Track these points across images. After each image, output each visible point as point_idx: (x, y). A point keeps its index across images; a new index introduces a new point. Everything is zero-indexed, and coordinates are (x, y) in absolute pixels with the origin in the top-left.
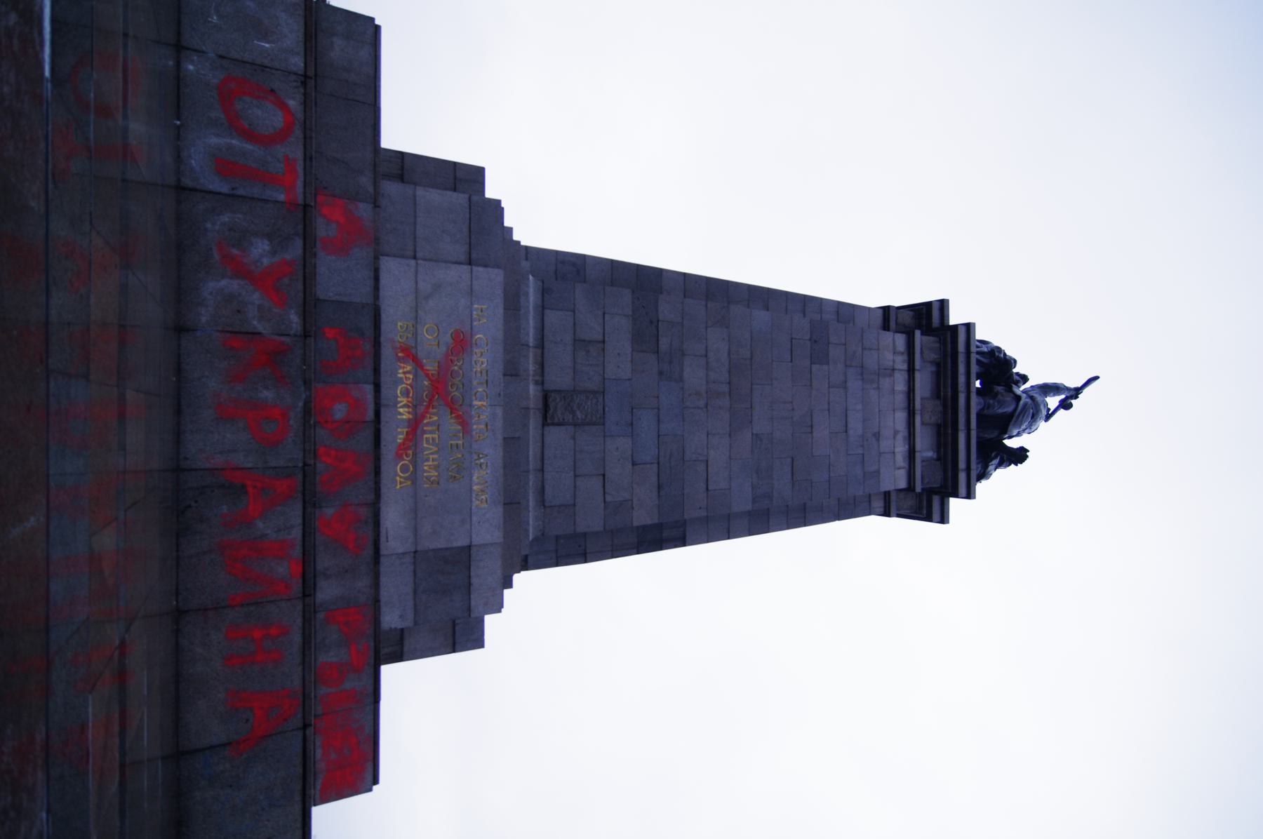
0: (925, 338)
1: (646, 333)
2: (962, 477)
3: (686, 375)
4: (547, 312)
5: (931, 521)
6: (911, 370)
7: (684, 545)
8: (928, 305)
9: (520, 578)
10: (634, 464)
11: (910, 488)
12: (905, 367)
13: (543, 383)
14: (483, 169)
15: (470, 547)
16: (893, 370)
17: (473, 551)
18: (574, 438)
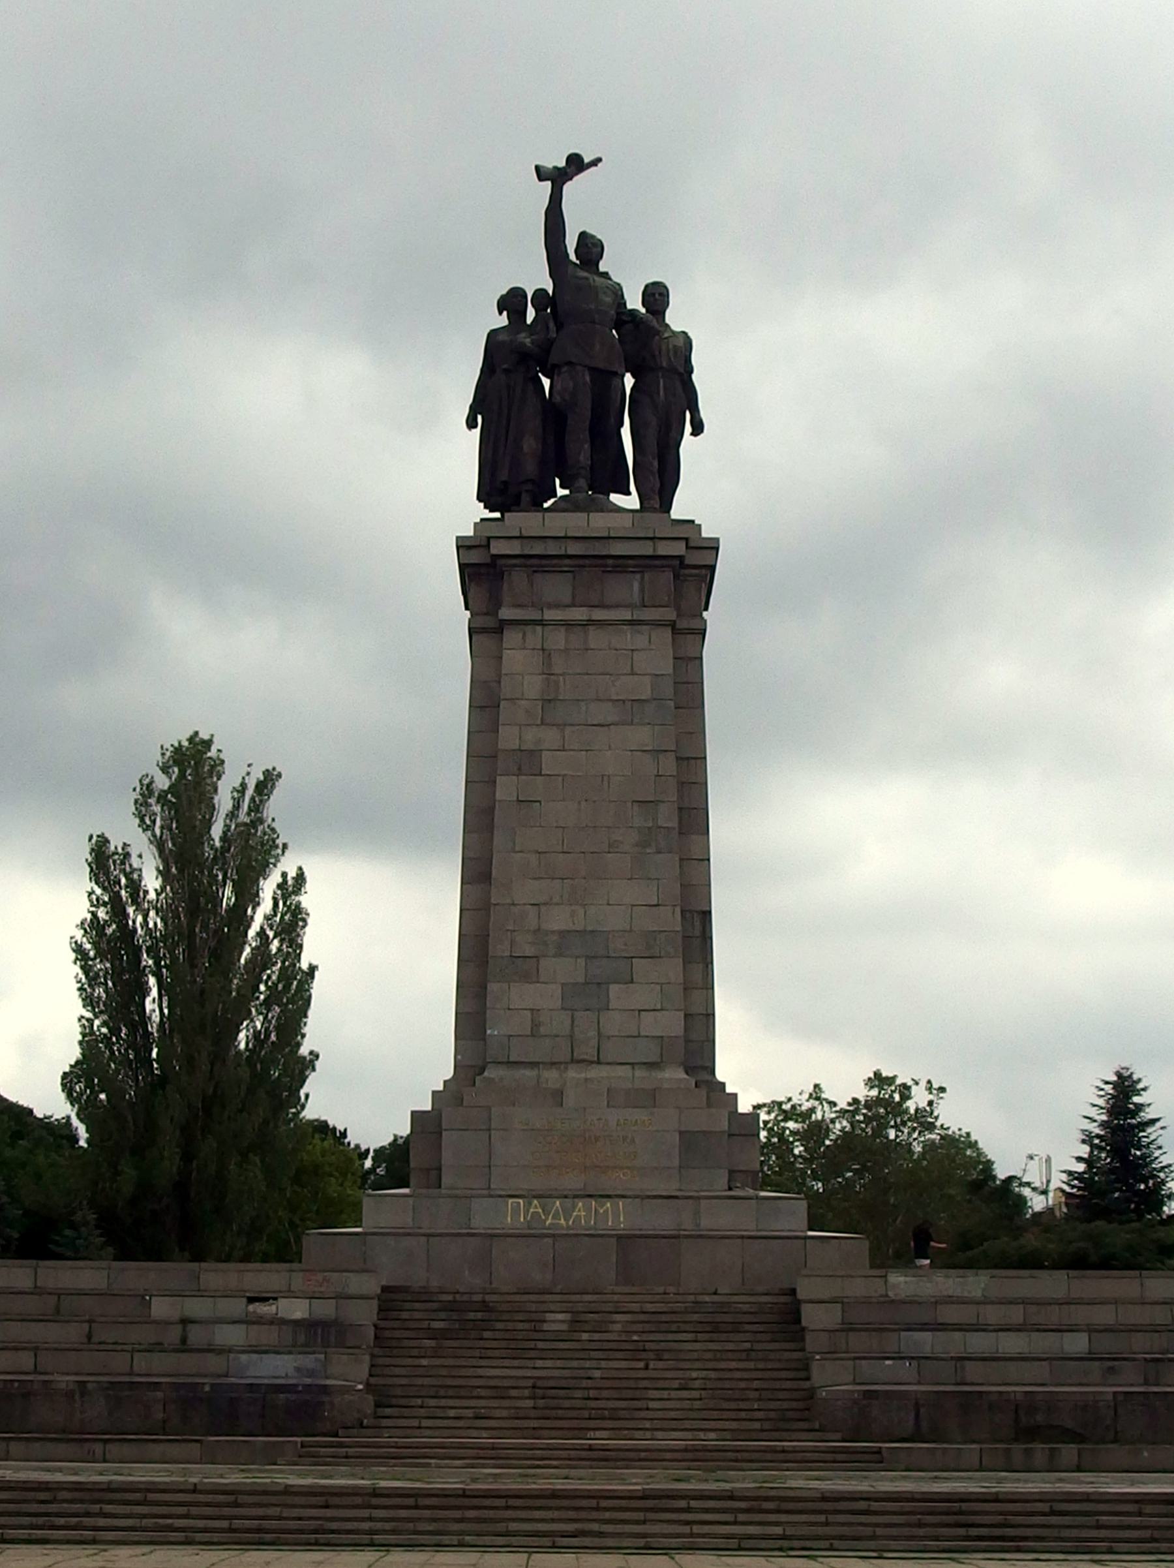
0: (507, 598)
1: (525, 970)
2: (664, 549)
3: (556, 927)
4: (511, 1059)
5: (712, 569)
6: (541, 623)
7: (709, 913)
8: (462, 567)
9: (720, 1075)
10: (632, 982)
11: (673, 625)
12: (539, 628)
13: (566, 1063)
14: (414, 1114)
15: (681, 1133)
16: (543, 649)
17: (683, 1129)
18: (608, 1037)
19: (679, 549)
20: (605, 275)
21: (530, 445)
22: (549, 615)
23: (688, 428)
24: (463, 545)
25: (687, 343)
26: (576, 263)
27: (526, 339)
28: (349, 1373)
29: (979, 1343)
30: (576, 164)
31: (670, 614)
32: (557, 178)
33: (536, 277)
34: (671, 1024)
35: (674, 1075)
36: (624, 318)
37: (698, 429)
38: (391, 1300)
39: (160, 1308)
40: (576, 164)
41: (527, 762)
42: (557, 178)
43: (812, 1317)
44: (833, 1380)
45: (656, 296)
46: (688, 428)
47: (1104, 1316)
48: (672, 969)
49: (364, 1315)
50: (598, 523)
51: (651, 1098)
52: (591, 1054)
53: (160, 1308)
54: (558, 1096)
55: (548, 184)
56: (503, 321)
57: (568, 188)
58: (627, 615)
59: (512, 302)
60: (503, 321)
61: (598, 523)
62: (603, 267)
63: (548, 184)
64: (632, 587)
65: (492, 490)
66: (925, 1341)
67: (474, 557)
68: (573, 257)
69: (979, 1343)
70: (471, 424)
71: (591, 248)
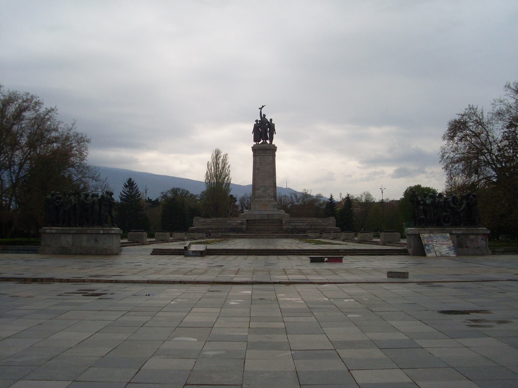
1: (258, 189)
21: (258, 136)
26: (263, 117)
27: (258, 125)
28: (244, 227)
29: (297, 224)
30: (263, 106)
32: (261, 109)
34: (272, 194)
35: (273, 199)
36: (268, 122)
38: (247, 221)
39: (228, 222)
40: (263, 106)
41: (258, 169)
42: (261, 109)
43: (283, 222)
44: (285, 227)
45: (271, 120)
47: (308, 222)
49: (245, 222)
50: (265, 145)
51: (271, 201)
53: (228, 222)
54: (262, 201)
59: (257, 121)
61: (265, 145)
64: (269, 151)
65: (255, 141)
66: (293, 224)
69: (297, 224)
71: (264, 115)
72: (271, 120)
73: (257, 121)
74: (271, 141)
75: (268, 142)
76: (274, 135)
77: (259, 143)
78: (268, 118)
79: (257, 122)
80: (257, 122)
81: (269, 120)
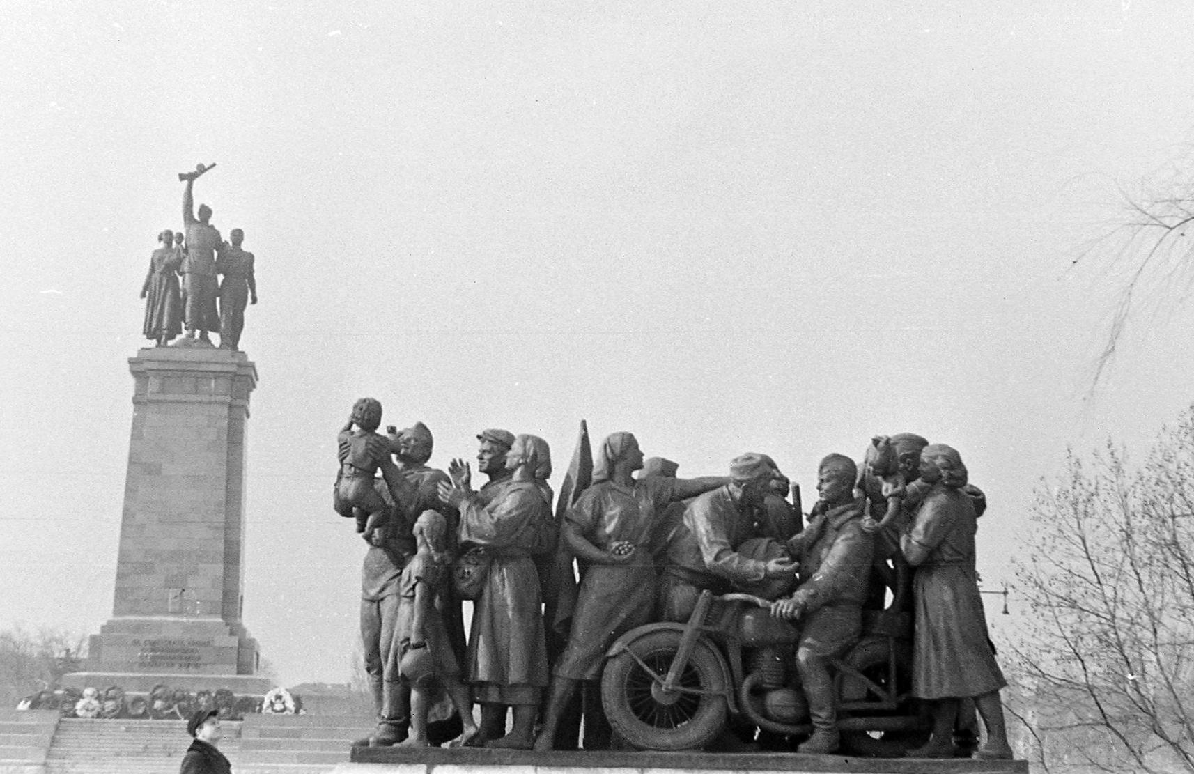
1: (147, 569)
19: (233, 368)
20: (212, 227)
22: (170, 397)
23: (250, 300)
24: (131, 362)
25: (251, 256)
30: (202, 170)
31: (228, 399)
32: (191, 178)
33: (179, 227)
36: (220, 246)
37: (254, 301)
40: (202, 170)
42: (191, 178)
45: (238, 235)
46: (250, 300)
48: (219, 569)
52: (177, 608)
55: (186, 182)
56: (161, 245)
57: (196, 183)
58: (205, 398)
60: (161, 245)
62: (211, 222)
63: (186, 182)
67: (136, 368)
68: (196, 216)
70: (143, 295)
71: (206, 212)
72: (238, 235)
73: (167, 237)
74: (232, 338)
75: (215, 338)
76: (249, 311)
77: (170, 343)
78: (224, 226)
79: (169, 244)
80: (169, 244)
81: (226, 237)
